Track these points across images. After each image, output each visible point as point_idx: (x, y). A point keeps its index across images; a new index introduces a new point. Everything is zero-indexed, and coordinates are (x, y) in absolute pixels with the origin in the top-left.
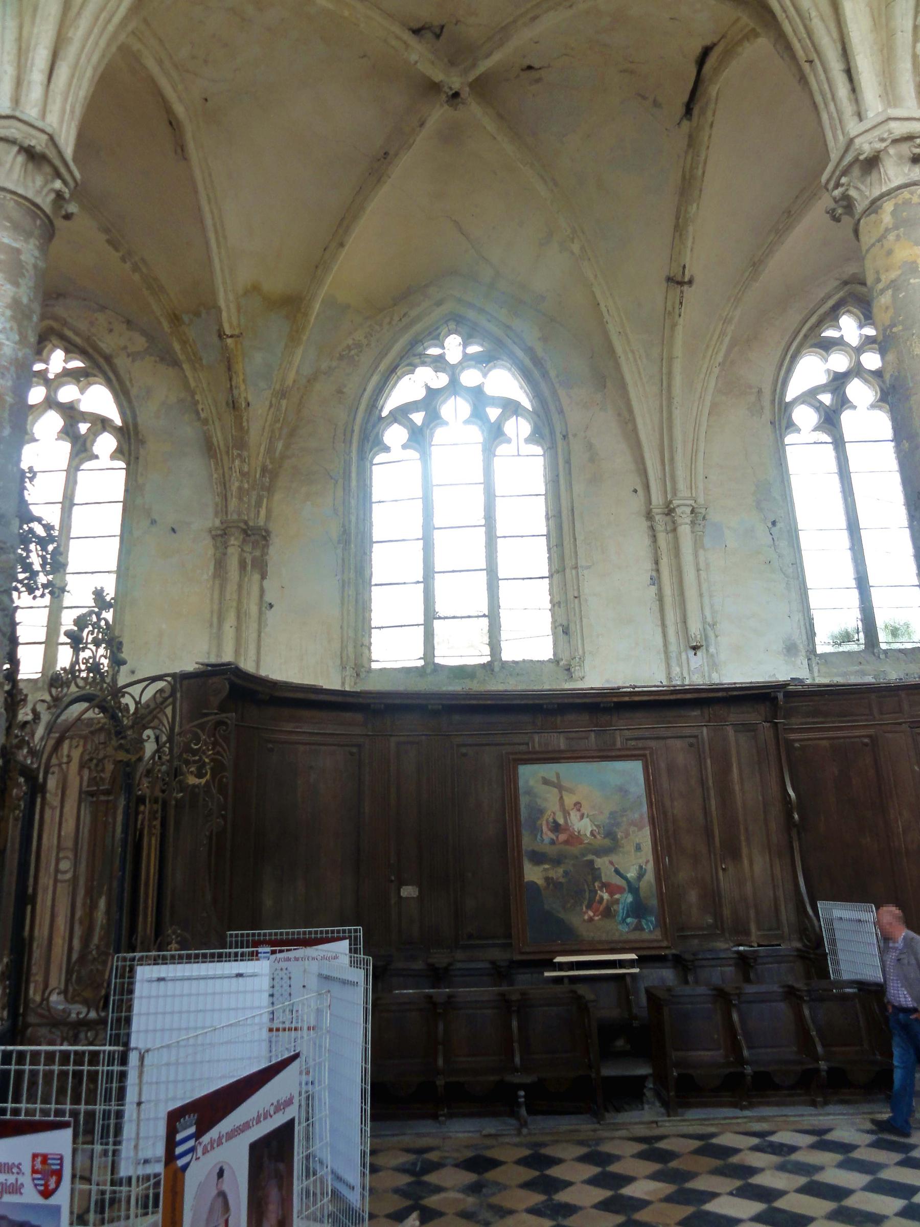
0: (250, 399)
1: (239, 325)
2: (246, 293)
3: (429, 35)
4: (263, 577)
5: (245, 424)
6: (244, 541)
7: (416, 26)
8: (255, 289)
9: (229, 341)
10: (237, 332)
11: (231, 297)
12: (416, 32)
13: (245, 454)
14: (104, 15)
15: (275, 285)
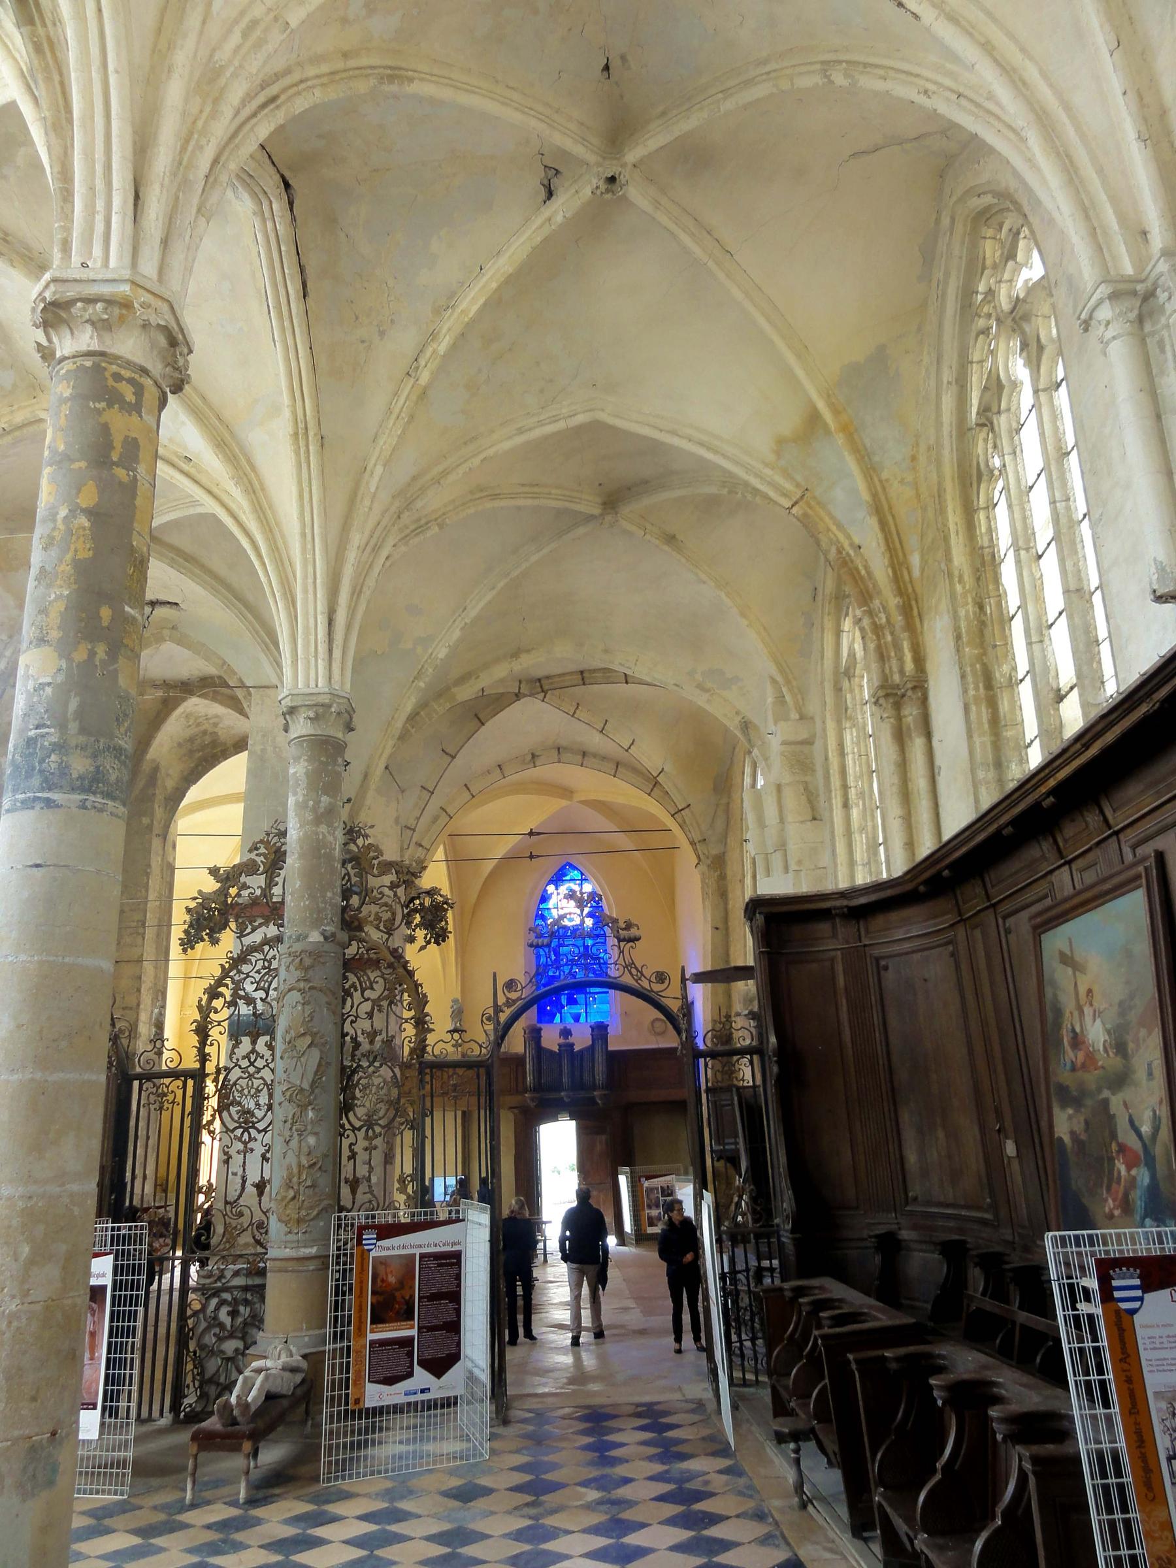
0: (857, 541)
1: (798, 485)
2: (778, 453)
3: (555, 181)
4: (928, 735)
5: (863, 572)
6: (897, 706)
7: (543, 193)
8: (781, 443)
9: (794, 511)
10: (799, 494)
11: (768, 471)
12: (550, 194)
13: (876, 603)
14: (310, 581)
15: (790, 422)
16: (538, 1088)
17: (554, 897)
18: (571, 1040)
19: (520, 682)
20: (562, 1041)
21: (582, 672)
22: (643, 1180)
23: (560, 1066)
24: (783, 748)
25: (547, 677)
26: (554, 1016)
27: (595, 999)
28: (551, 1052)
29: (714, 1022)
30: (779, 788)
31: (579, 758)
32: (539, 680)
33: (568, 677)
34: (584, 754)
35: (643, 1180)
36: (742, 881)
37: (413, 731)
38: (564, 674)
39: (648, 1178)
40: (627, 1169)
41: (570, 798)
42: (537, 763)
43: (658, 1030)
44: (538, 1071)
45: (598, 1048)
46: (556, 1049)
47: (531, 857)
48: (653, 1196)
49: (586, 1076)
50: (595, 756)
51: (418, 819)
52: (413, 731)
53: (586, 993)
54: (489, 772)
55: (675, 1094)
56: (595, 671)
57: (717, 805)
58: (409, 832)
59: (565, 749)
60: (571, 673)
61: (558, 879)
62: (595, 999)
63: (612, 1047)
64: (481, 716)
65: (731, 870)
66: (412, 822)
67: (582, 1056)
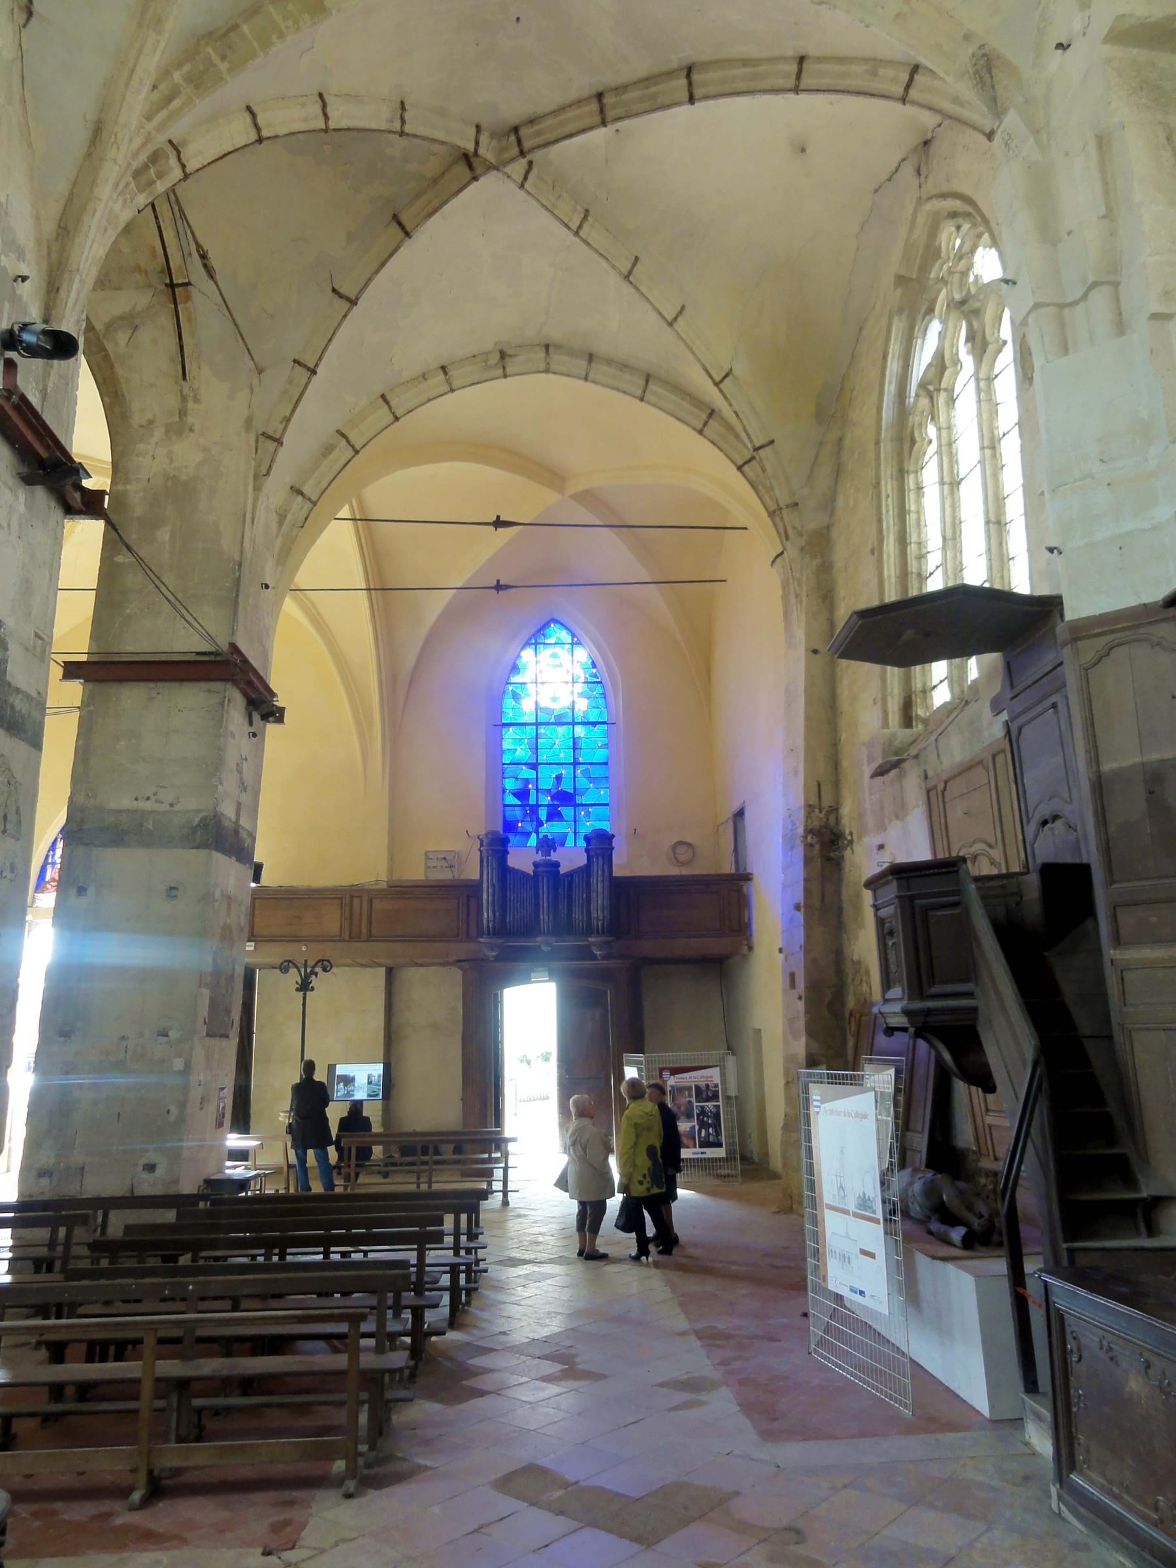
16: (502, 930)
17: (532, 665)
18: (554, 857)
19: (478, 128)
20: (539, 857)
21: (600, 96)
22: (666, 1074)
23: (537, 896)
24: (1108, 50)
25: (532, 121)
26: (528, 834)
27: (588, 814)
28: (523, 875)
29: (809, 808)
30: (1103, 142)
31: (584, 363)
32: (516, 130)
33: (570, 114)
34: (591, 358)
35: (666, 1074)
36: (877, 551)
37: (223, 66)
38: (562, 109)
39: (675, 1071)
40: (640, 1057)
41: (561, 490)
42: (509, 370)
43: (682, 858)
44: (502, 902)
45: (597, 870)
46: (530, 870)
47: (499, 587)
48: (683, 1100)
49: (577, 915)
50: (609, 362)
51: (288, 420)
52: (223, 66)
53: (576, 806)
54: (424, 377)
55: (711, 946)
56: (623, 88)
57: (821, 444)
58: (271, 446)
59: (558, 347)
60: (579, 102)
61: (536, 638)
62: (588, 814)
63: (617, 872)
64: (404, 219)
65: (839, 556)
66: (275, 428)
67: (570, 883)
